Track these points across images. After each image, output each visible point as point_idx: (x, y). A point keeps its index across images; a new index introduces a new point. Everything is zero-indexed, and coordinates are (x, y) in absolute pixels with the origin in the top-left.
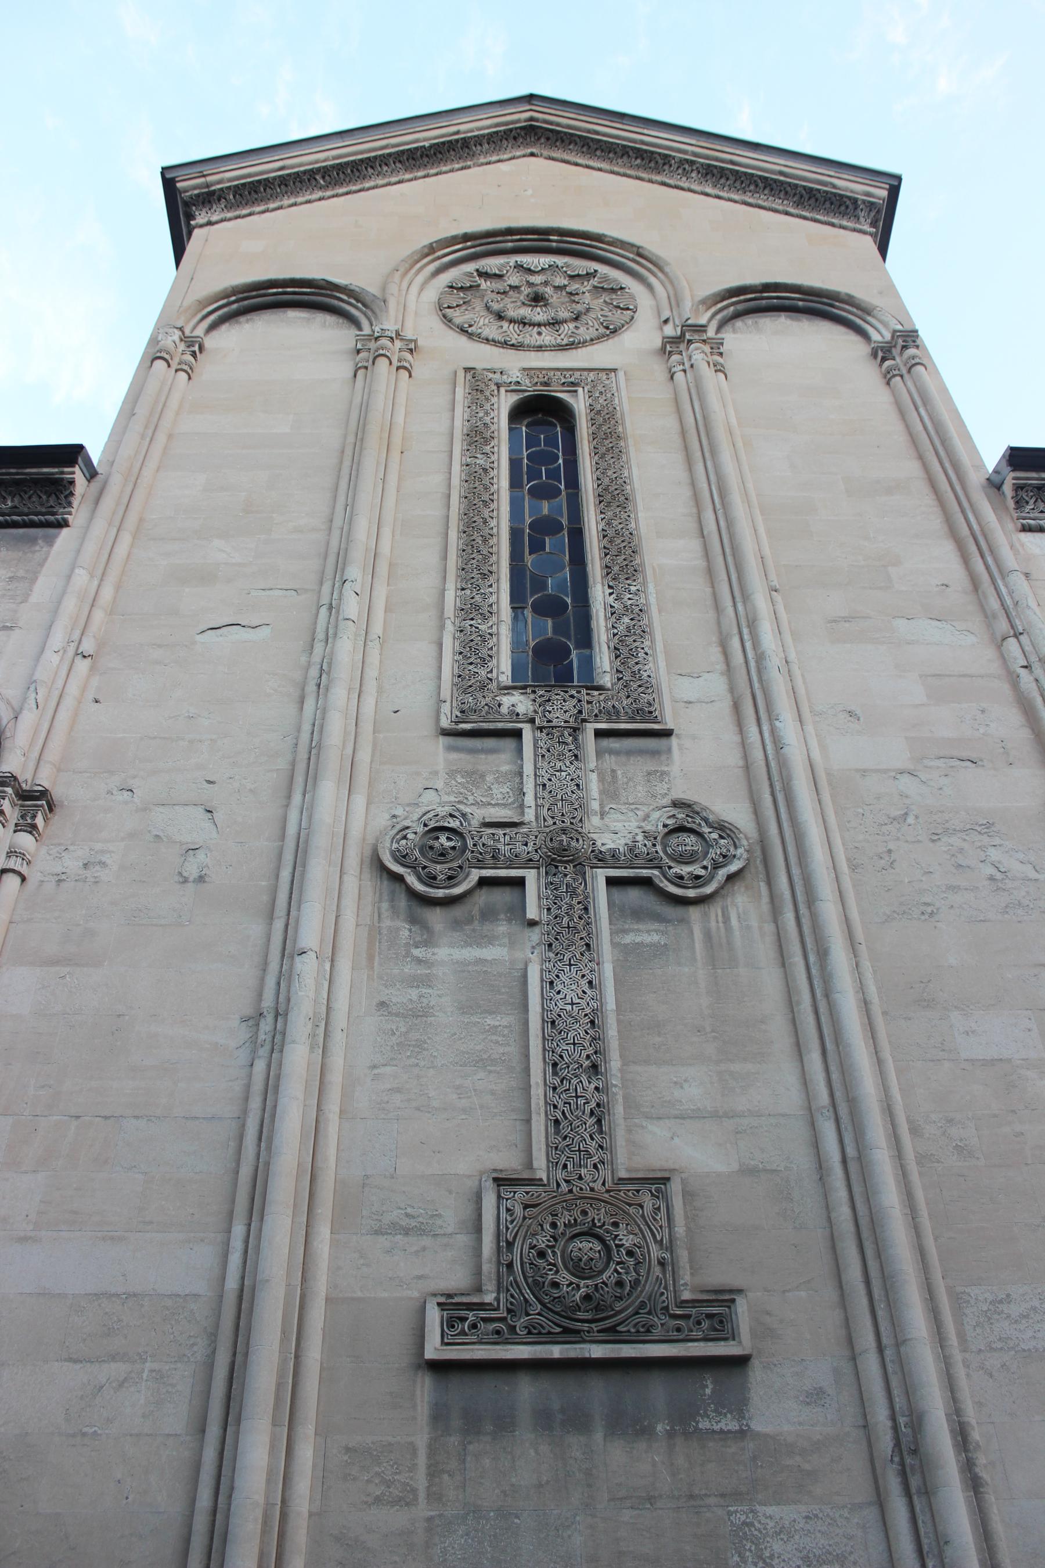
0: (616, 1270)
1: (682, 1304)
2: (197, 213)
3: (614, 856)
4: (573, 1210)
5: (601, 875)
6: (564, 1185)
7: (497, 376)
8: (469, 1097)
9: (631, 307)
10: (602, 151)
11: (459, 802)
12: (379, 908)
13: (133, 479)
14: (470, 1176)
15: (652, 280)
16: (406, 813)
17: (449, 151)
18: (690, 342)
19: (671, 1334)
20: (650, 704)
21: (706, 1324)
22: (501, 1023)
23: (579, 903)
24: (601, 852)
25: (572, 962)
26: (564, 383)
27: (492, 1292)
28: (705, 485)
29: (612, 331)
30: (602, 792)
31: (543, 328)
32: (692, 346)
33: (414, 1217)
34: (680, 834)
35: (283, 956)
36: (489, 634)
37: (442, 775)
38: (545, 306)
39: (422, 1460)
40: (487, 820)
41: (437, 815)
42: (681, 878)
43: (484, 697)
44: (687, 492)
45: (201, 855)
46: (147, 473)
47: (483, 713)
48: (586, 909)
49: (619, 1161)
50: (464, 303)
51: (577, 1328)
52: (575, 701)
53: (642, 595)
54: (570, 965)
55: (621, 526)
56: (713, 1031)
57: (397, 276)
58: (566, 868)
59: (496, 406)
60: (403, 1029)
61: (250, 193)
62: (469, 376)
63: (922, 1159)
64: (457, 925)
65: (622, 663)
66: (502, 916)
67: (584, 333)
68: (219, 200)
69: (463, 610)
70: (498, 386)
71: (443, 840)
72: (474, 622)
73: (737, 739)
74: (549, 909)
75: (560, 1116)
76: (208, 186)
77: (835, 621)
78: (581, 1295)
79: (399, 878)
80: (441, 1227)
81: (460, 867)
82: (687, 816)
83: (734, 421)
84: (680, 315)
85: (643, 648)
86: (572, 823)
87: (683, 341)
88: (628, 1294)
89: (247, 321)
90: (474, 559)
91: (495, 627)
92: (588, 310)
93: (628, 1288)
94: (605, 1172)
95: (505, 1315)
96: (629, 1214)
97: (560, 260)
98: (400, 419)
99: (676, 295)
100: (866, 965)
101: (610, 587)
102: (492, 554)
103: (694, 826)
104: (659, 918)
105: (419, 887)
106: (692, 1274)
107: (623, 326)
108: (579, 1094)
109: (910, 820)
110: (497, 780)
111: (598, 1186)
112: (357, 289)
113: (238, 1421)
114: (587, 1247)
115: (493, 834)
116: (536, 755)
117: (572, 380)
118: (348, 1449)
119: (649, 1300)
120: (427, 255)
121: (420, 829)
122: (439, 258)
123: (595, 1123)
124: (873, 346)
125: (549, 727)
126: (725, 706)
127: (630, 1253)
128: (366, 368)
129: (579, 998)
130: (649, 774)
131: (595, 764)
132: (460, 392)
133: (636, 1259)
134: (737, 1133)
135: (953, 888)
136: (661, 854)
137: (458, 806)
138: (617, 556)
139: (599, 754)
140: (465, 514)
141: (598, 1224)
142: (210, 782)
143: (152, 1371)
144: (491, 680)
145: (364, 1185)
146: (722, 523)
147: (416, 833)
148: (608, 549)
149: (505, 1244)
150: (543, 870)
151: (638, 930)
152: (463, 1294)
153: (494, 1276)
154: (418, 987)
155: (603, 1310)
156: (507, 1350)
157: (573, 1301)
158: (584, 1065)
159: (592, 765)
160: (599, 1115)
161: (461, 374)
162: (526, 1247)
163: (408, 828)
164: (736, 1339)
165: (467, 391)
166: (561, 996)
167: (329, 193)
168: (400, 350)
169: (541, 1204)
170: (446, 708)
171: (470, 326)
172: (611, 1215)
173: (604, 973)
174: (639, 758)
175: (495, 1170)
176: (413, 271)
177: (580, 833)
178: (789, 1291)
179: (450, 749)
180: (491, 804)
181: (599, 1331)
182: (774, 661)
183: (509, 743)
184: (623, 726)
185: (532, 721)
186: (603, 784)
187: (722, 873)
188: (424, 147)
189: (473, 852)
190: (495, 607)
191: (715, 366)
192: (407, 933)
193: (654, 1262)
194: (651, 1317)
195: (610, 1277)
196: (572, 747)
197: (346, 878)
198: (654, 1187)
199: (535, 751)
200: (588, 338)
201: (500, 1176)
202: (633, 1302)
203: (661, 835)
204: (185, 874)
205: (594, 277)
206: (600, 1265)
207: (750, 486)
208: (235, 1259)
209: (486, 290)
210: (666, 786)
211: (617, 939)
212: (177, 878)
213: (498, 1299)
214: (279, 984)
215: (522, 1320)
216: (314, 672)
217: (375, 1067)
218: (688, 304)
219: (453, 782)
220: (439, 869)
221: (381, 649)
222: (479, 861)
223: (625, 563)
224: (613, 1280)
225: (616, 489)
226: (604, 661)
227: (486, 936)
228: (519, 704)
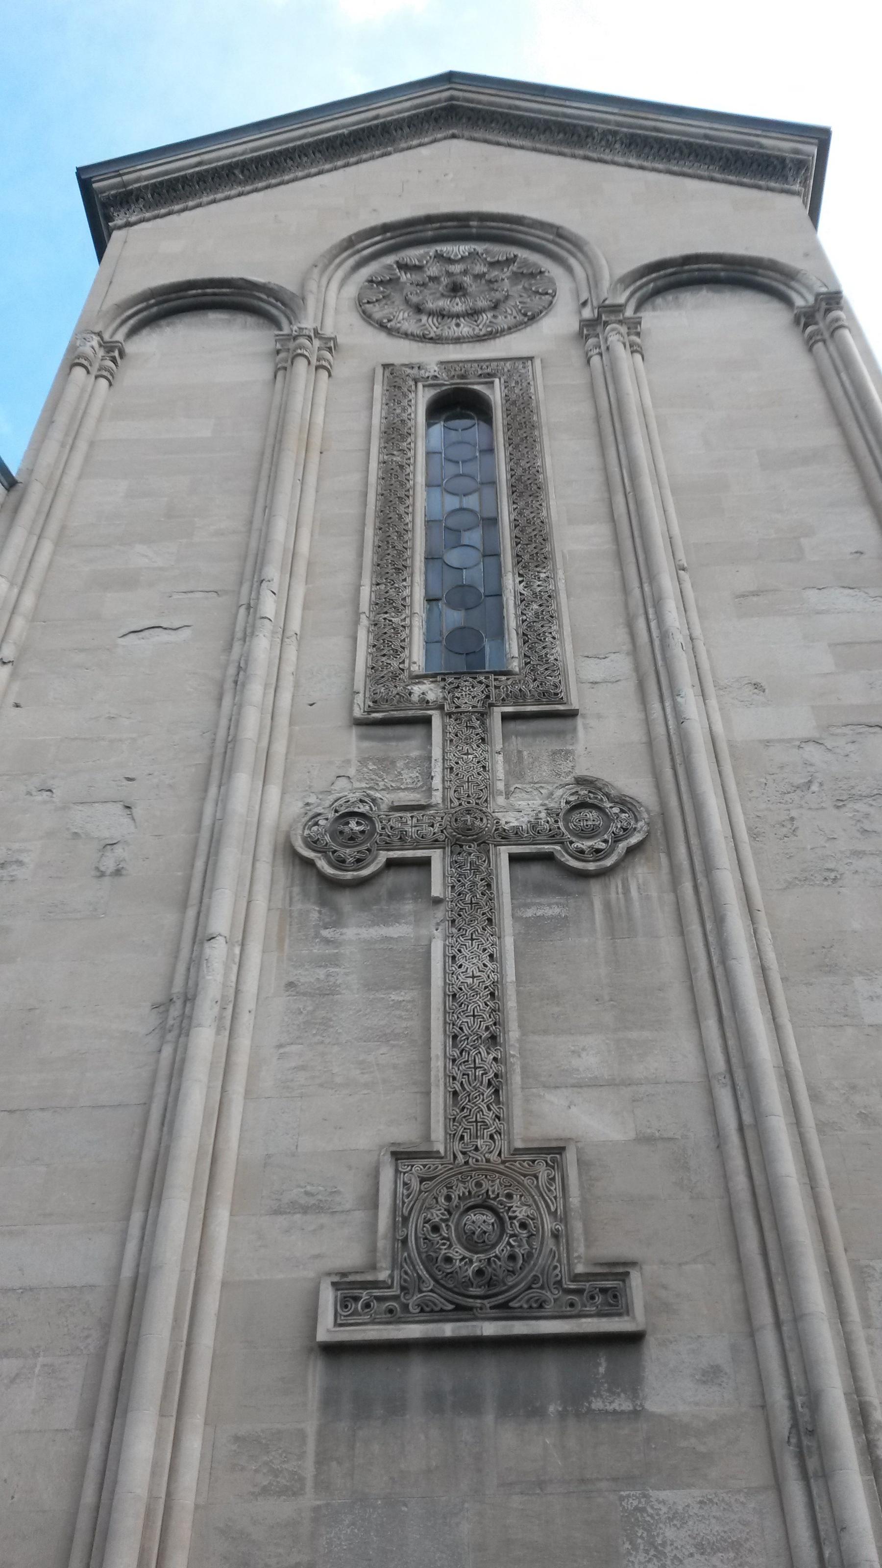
0: (509, 1243)
1: (576, 1278)
2: (115, 214)
3: (517, 833)
4: (468, 1181)
5: (504, 852)
6: (460, 1157)
7: (415, 371)
9: (550, 291)
10: (525, 127)
11: (371, 788)
12: (291, 892)
13: (54, 487)
14: (370, 1151)
15: (572, 261)
16: (319, 801)
17: (368, 137)
18: (606, 324)
19: (564, 1309)
20: (557, 687)
21: (599, 1299)
22: (405, 998)
23: (482, 880)
24: (504, 830)
25: (474, 937)
26: (481, 375)
27: (386, 1269)
28: (617, 469)
29: (531, 318)
30: (507, 773)
31: (462, 319)
32: (608, 328)
33: (312, 1195)
34: (582, 810)
35: (194, 943)
36: (402, 626)
37: (355, 763)
38: (464, 295)
39: (311, 1447)
40: (396, 804)
41: (348, 801)
42: (582, 852)
43: (396, 686)
44: (597, 478)
45: (119, 850)
46: (69, 481)
47: (395, 702)
48: (489, 886)
49: (515, 1131)
50: (384, 297)
51: (469, 1305)
52: (483, 686)
53: (552, 581)
54: (472, 939)
55: (533, 515)
57: (316, 271)
58: (470, 847)
59: (413, 402)
60: (310, 1008)
61: (168, 191)
62: (387, 373)
64: (364, 906)
65: (530, 648)
66: (409, 895)
67: (502, 322)
68: (137, 200)
69: (377, 604)
70: (416, 381)
71: (353, 824)
72: (388, 615)
73: (641, 716)
74: (453, 887)
75: (458, 1087)
76: (124, 185)
77: (743, 596)
79: (309, 863)
80: (340, 1204)
81: (369, 850)
82: (590, 792)
83: (648, 402)
84: (598, 298)
85: (551, 633)
86: (477, 804)
87: (601, 323)
88: (521, 1268)
89: (168, 325)
90: (389, 554)
91: (408, 620)
92: (507, 297)
93: (521, 1262)
94: (501, 1143)
95: (398, 1292)
96: (523, 1185)
97: (480, 247)
98: (319, 418)
99: (595, 276)
101: (520, 575)
102: (406, 549)
103: (596, 802)
104: (560, 892)
105: (329, 870)
106: (588, 1247)
107: (541, 312)
108: (477, 1065)
110: (407, 766)
111: (493, 1157)
112: (276, 288)
113: (125, 1412)
114: (482, 1220)
115: (401, 818)
116: (444, 740)
117: (489, 370)
118: (237, 1439)
119: (542, 1274)
120: (346, 249)
121: (331, 815)
122: (358, 251)
123: (493, 1093)
124: (795, 311)
125: (458, 713)
126: (629, 686)
127: (523, 1225)
128: (285, 369)
129: (479, 971)
130: (554, 753)
131: (502, 746)
132: (378, 389)
133: (529, 1231)
134: (634, 1101)
136: (563, 829)
137: (369, 792)
138: (527, 545)
139: (505, 737)
140: (382, 511)
141: (492, 1196)
142: (129, 779)
143: (44, 1365)
144: (403, 670)
146: (632, 507)
147: (327, 819)
148: (519, 538)
149: (400, 1219)
150: (448, 850)
151: (540, 904)
152: (357, 1272)
153: (389, 1252)
154: (326, 966)
156: (399, 1330)
157: (466, 1276)
158: (483, 1037)
159: (499, 746)
160: (497, 1085)
161: (379, 371)
162: (421, 1221)
163: (319, 814)
164: (631, 1315)
165: (385, 388)
166: (463, 969)
167: (248, 188)
168: (319, 349)
169: (438, 1176)
170: (359, 699)
171: (389, 321)
172: (506, 1186)
173: (505, 946)
174: (545, 739)
175: (393, 1144)
176: (332, 267)
177: (484, 813)
178: (686, 1263)
179: (362, 738)
180: (401, 789)
181: (491, 1308)
182: (678, 638)
183: (419, 731)
184: (529, 708)
185: (441, 708)
186: (509, 766)
187: (622, 846)
188: (343, 134)
189: (381, 835)
190: (408, 600)
191: (631, 346)
193: (548, 1234)
194: (544, 1292)
195: (503, 1250)
196: (479, 731)
197: (258, 865)
198: (549, 1157)
199: (443, 736)
200: (506, 327)
201: (398, 1150)
202: (526, 1277)
203: (563, 811)
204: (102, 869)
205: (514, 263)
206: (493, 1238)
207: (662, 466)
209: (405, 283)
210: (571, 764)
211: (519, 914)
212: (94, 873)
213: (391, 1276)
214: (189, 969)
215: (415, 1298)
216: (232, 671)
217: (281, 1046)
218: (606, 283)
220: (348, 853)
221: (299, 645)
223: (535, 551)
224: (506, 1253)
225: (529, 479)
226: (513, 646)
228: (429, 692)
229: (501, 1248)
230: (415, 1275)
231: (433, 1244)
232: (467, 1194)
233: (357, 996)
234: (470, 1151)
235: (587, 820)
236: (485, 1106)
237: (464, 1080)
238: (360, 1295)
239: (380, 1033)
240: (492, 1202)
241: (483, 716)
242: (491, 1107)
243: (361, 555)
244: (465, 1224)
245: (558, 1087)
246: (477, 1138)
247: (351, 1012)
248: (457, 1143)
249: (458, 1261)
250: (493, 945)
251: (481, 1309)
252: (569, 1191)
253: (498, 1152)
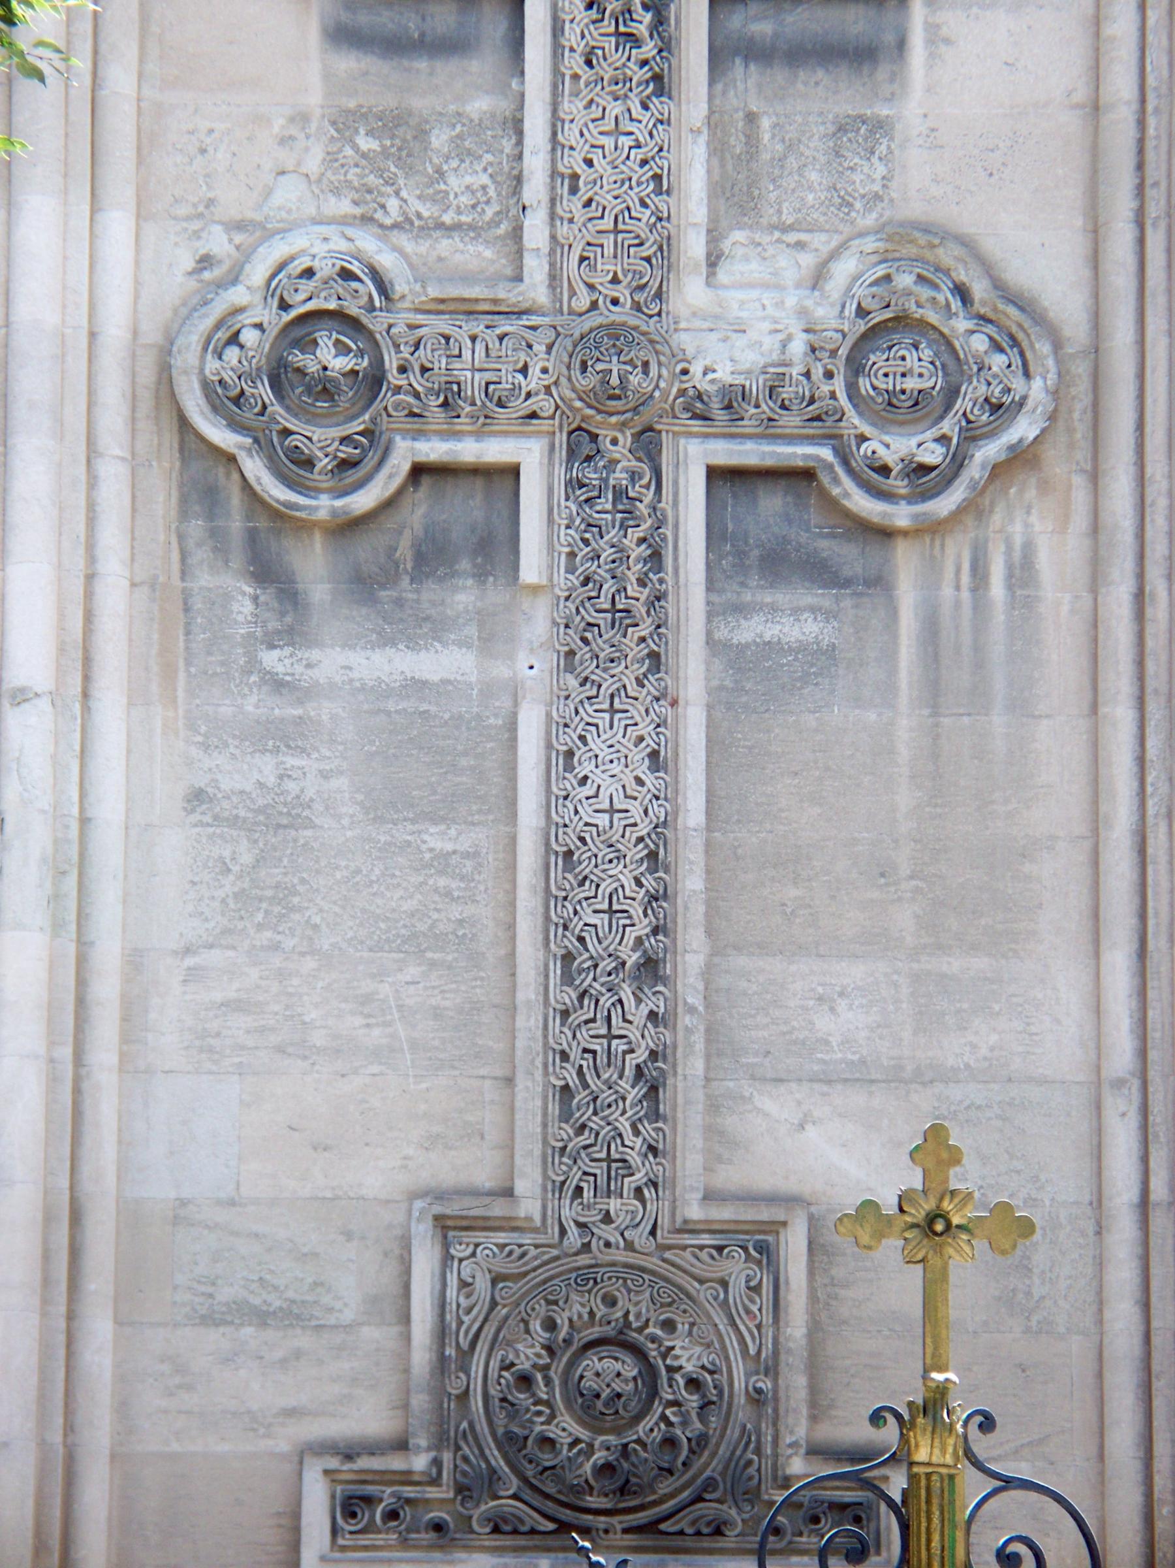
0: (664, 1418)
4: (589, 1292)
6: (573, 1231)
8: (388, 1024)
12: (181, 537)
14: (388, 1202)
25: (617, 705)
42: (884, 470)
54: (613, 711)
56: (911, 877)
66: (465, 564)
75: (573, 1080)
78: (595, 1465)
80: (331, 1310)
88: (684, 1464)
93: (685, 1452)
105: (276, 492)
106: (814, 1419)
108: (615, 1032)
111: (639, 1237)
121: (275, 320)
127: (693, 1383)
139: (718, 58)
141: (634, 1325)
145: (176, 1221)
151: (774, 609)
155: (635, 1493)
157: (580, 1476)
162: (494, 1364)
166: (588, 790)
169: (526, 1274)
172: (662, 1305)
174: (820, 73)
180: (440, 226)
181: (626, 1531)
189: (398, 390)
192: (248, 607)
195: (652, 1430)
210: (881, 170)
211: (721, 634)
213: (437, 1463)
217: (188, 951)
219: (348, 151)
222: (412, 414)
227: (427, 619)
229: (648, 1427)
230: (484, 1466)
231: (517, 1411)
232: (586, 1317)
233: (349, 834)
234: (593, 1223)
235: (903, 375)
236: (627, 1125)
237: (584, 1063)
238: (380, 1495)
239: (403, 931)
240: (635, 1335)
242: (640, 1127)
244: (582, 1377)
245: (781, 1080)
246: (609, 1197)
247: (338, 875)
248: (568, 1202)
249: (566, 1447)
250: (658, 726)
251: (606, 1531)
252: (786, 1312)
253: (649, 1227)
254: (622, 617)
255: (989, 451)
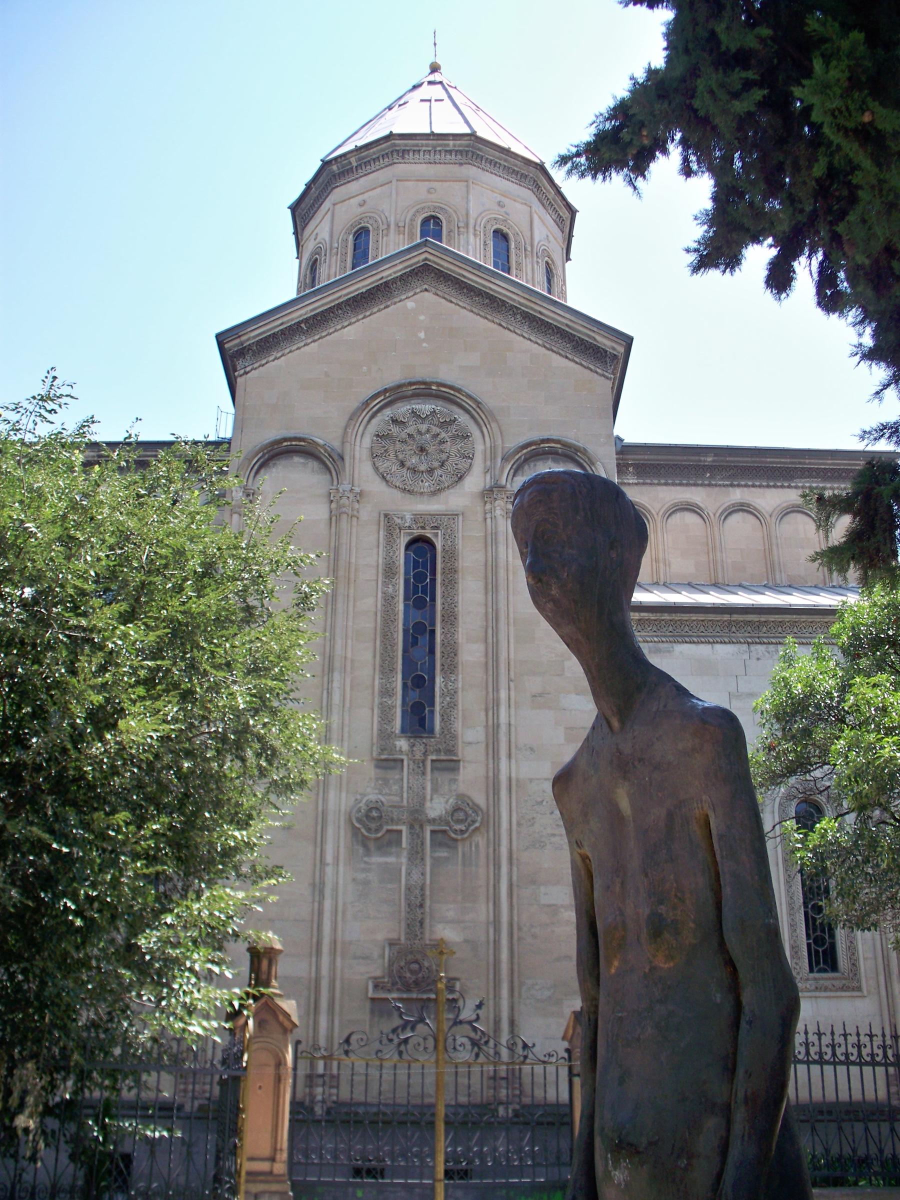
63: (519, 939)
100: (515, 869)
104: (449, 847)
105: (366, 834)
109: (544, 803)
126: (484, 745)
135: (554, 835)
139: (432, 770)
170: (375, 748)
208: (314, 969)
220: (373, 826)
241: (424, 762)
243: (375, 656)
254: (417, 853)
255: (472, 828)
